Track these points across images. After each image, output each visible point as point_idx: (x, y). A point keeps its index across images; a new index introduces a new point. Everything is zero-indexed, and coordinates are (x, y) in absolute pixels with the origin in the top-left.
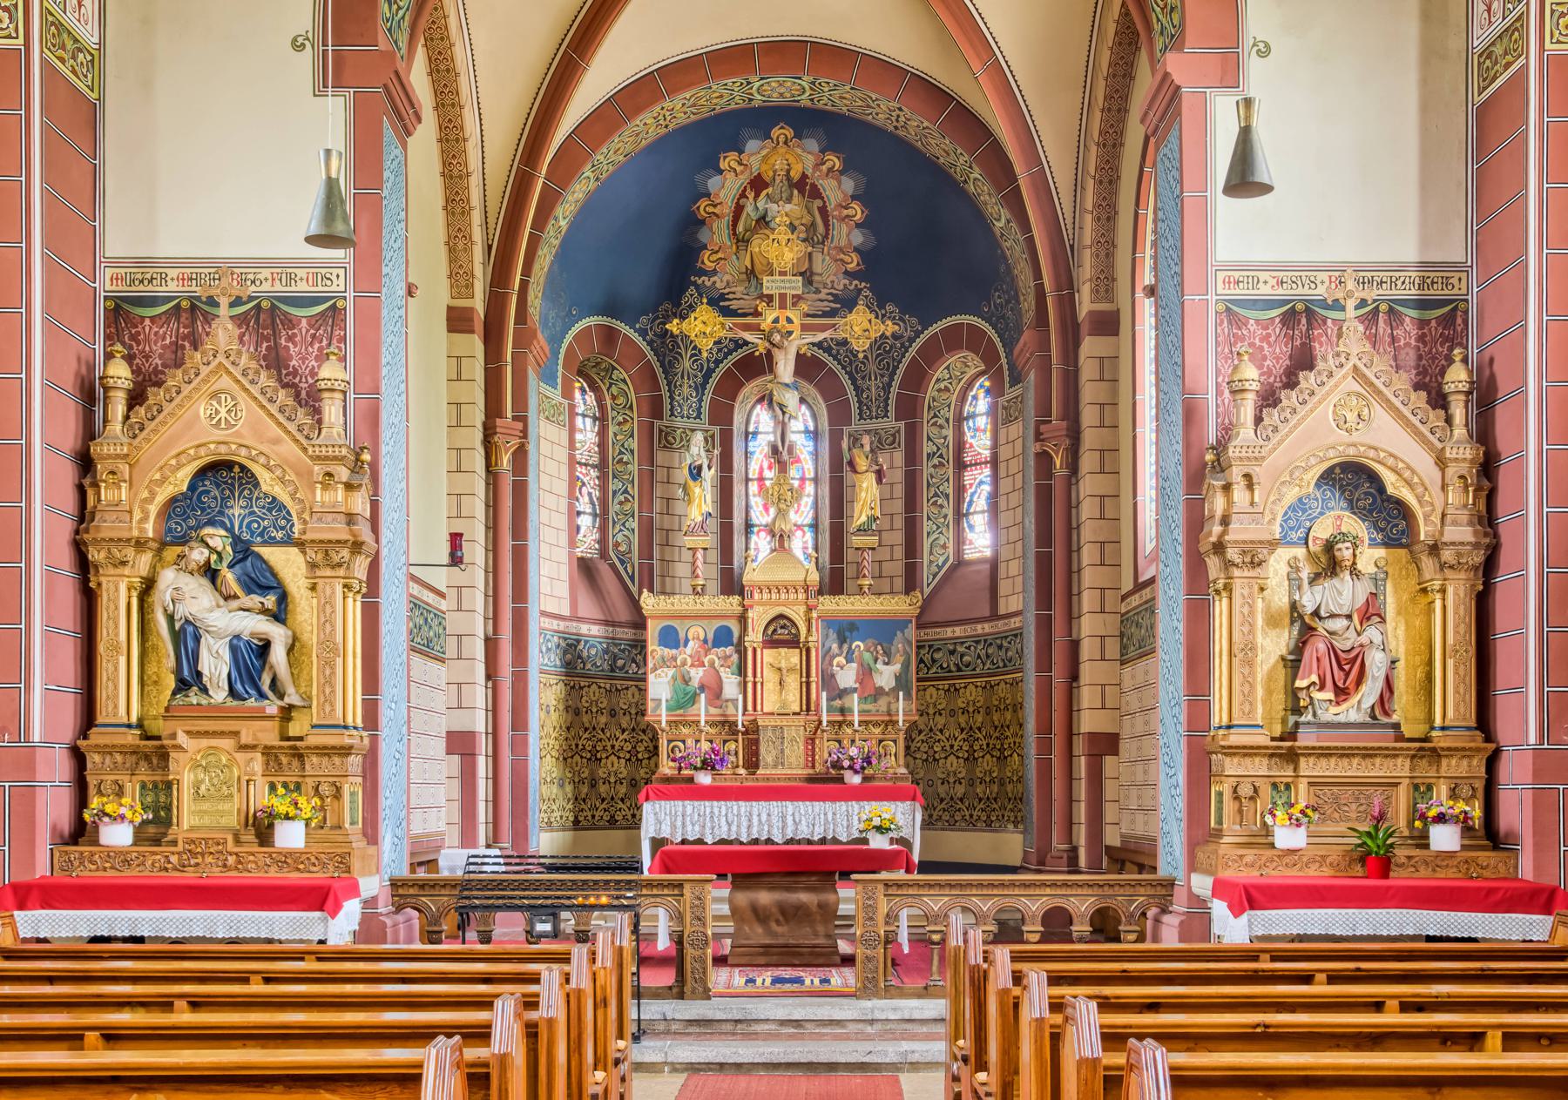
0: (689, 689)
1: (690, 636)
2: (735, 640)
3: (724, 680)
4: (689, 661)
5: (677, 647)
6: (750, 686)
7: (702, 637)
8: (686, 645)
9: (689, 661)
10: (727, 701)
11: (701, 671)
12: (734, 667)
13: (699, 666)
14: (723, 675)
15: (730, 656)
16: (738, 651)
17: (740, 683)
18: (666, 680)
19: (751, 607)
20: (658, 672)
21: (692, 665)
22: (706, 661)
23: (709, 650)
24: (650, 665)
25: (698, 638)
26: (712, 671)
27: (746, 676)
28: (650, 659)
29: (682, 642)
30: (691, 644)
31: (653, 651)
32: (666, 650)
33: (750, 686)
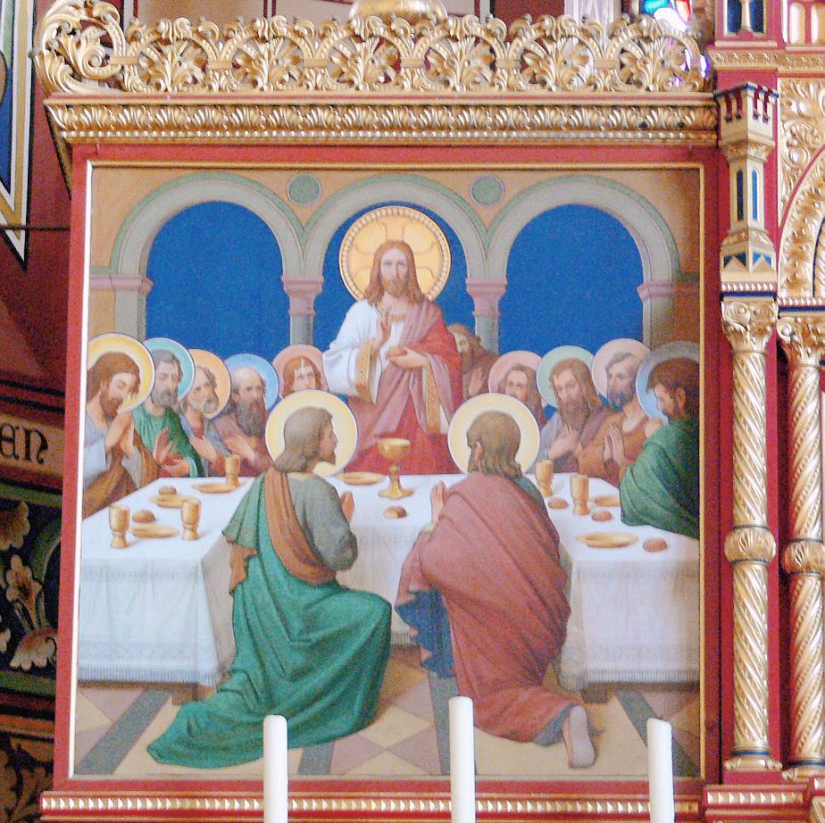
0: (338, 611)
1: (356, 270)
2: (652, 304)
3: (579, 555)
4: (346, 434)
5: (267, 342)
6: (753, 587)
7: (432, 275)
8: (324, 333)
9: (346, 434)
10: (596, 693)
11: (421, 495)
12: (646, 474)
13: (413, 464)
14: (570, 524)
15: (618, 403)
16: (678, 378)
17: (684, 573)
18: (186, 552)
19: (766, 82)
20: (138, 501)
21: (367, 460)
22: (458, 433)
23: (481, 359)
24: (88, 460)
25: (408, 288)
26: (497, 484)
27: (724, 521)
28: (85, 412)
29: (300, 311)
30: (359, 321)
31: (103, 372)
32: (197, 363)
33: (753, 587)
